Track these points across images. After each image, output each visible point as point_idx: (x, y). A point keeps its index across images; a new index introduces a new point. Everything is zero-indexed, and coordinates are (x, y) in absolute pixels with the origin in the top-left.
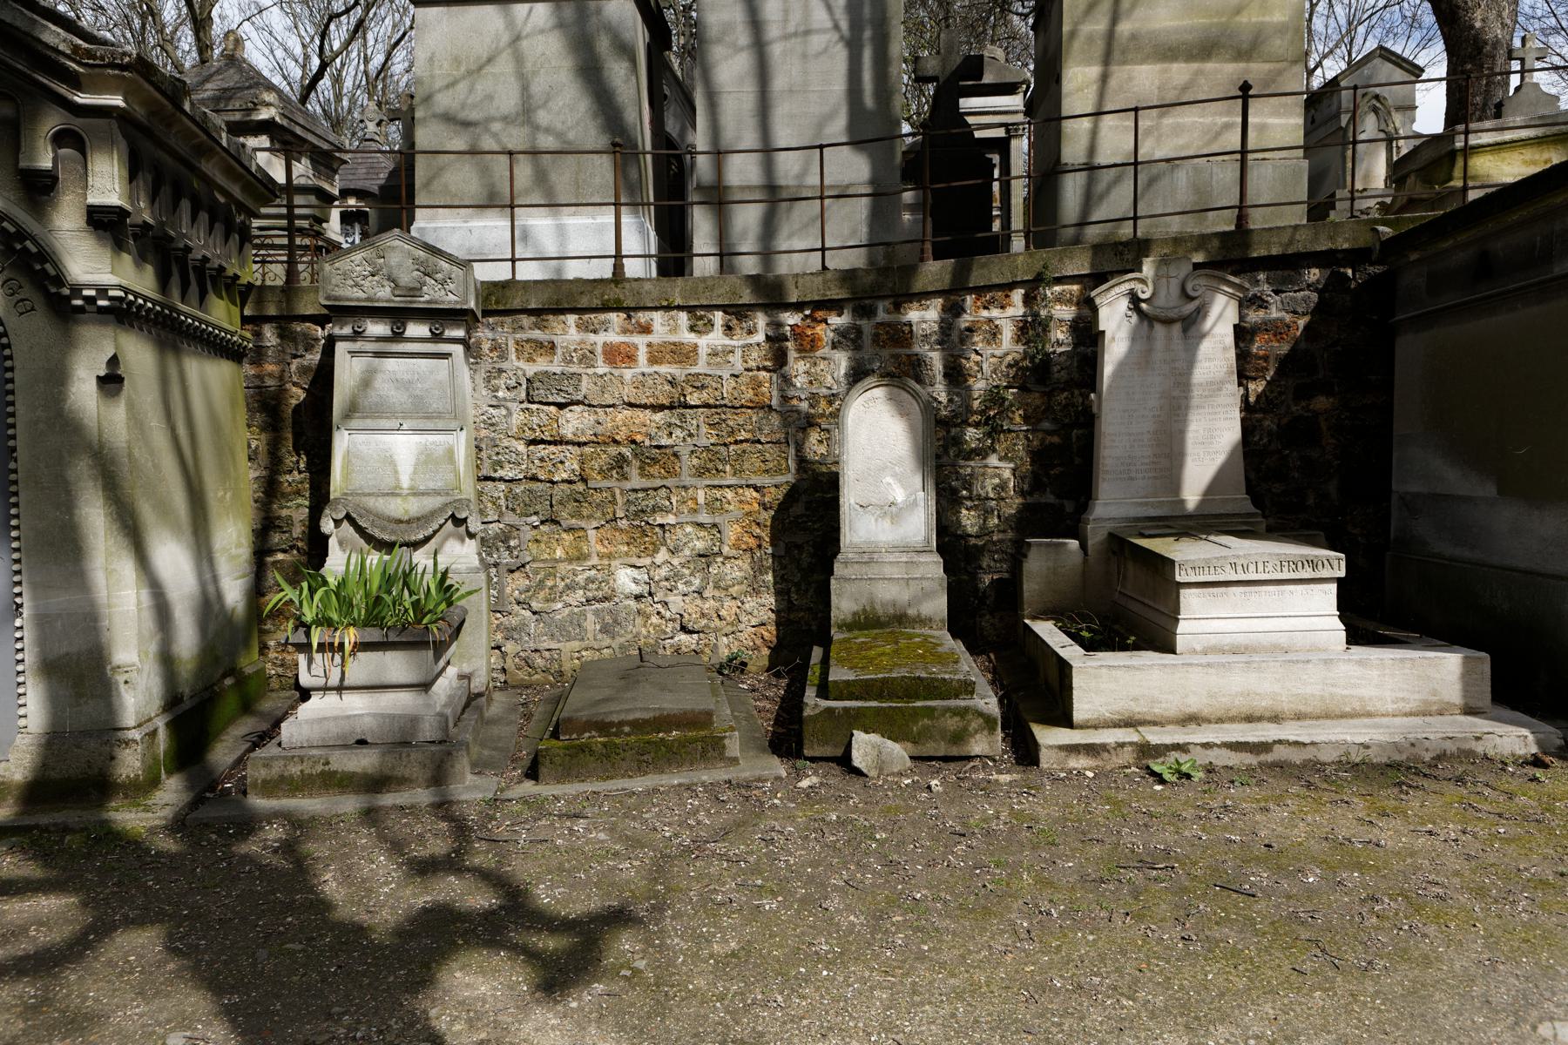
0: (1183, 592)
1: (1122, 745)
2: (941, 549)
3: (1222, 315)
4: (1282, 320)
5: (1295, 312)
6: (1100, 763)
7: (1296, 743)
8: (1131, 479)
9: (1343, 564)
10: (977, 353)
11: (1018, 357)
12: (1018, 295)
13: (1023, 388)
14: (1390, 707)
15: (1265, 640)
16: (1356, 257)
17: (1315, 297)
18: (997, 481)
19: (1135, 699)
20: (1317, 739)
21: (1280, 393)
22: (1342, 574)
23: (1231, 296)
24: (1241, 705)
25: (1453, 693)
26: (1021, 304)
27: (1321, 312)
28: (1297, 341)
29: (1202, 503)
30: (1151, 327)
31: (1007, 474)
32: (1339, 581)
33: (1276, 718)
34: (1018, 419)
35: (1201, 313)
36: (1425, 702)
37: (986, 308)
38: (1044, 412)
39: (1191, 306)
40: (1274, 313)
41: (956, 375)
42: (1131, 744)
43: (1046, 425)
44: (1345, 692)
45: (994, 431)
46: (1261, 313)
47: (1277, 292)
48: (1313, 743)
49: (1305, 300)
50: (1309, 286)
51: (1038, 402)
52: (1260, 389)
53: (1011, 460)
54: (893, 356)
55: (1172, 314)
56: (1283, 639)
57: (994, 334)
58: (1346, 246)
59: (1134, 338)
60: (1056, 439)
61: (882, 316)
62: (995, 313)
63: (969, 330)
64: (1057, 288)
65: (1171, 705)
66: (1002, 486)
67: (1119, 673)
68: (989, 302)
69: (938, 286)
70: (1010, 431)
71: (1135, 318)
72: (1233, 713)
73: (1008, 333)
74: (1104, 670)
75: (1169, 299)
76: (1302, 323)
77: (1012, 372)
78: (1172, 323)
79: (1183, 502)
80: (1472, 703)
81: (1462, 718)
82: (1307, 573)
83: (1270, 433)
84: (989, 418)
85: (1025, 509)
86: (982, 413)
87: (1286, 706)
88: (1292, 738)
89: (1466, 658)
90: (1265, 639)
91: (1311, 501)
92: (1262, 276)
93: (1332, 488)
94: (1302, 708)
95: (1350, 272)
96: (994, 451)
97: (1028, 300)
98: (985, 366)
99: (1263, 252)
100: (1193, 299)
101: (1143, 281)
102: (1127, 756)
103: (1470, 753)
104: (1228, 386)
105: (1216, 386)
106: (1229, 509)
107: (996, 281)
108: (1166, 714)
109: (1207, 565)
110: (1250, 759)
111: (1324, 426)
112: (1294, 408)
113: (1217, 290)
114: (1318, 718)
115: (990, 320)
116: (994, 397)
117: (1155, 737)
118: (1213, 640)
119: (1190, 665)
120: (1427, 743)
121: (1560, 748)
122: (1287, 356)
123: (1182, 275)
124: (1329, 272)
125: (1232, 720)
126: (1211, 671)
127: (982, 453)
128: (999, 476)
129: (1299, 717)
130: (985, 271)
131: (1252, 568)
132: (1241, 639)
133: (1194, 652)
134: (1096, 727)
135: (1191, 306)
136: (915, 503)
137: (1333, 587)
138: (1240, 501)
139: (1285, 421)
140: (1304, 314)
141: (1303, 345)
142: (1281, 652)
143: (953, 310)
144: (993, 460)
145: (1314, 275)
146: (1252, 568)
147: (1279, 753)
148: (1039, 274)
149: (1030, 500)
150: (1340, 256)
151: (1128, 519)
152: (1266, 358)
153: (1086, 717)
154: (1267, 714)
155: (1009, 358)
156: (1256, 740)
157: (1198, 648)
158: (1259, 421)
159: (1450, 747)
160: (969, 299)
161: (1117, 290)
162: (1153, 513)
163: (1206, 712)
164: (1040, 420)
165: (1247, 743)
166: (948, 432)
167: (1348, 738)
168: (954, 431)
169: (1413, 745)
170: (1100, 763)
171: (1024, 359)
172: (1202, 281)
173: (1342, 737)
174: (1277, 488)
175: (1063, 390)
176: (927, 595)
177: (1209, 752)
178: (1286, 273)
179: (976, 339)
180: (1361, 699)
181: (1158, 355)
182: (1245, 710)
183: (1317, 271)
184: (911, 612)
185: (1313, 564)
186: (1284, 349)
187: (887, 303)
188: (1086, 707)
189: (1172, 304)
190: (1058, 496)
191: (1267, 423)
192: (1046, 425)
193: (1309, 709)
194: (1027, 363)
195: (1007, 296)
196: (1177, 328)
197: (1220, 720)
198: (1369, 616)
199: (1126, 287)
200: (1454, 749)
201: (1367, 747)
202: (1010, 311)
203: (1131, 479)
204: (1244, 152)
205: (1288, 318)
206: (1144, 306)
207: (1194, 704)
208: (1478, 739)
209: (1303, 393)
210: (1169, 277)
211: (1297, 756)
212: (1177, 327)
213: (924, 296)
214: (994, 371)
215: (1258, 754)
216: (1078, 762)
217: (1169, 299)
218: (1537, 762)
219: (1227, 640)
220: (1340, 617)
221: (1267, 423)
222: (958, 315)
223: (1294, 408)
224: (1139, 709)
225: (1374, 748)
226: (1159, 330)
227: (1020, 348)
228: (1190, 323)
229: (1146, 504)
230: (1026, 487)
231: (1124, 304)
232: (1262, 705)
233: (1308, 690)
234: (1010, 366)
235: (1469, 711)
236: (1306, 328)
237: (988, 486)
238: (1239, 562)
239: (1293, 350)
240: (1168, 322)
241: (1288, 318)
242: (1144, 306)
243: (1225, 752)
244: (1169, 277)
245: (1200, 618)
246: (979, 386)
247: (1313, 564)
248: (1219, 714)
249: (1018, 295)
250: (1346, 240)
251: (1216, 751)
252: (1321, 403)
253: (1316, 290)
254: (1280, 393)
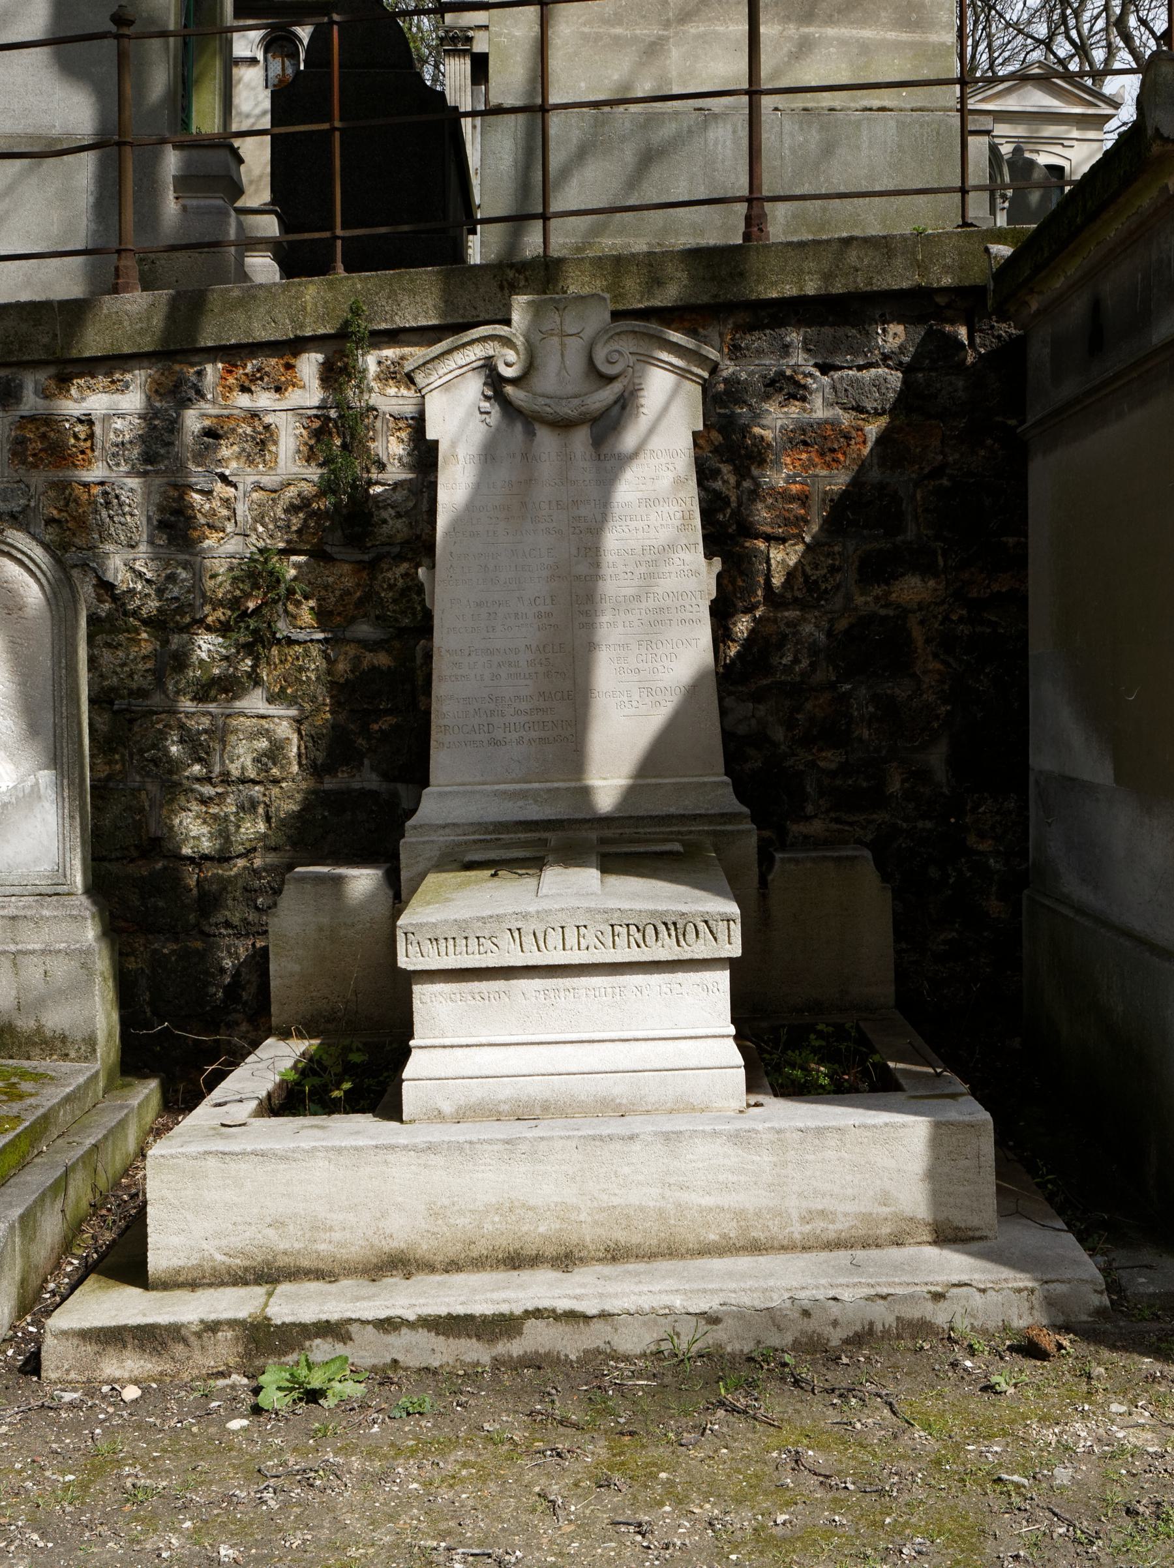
0: (417, 989)
1: (212, 1327)
2: (100, 886)
3: (667, 410)
4: (833, 423)
5: (859, 409)
6: (169, 1367)
7: (572, 1316)
8: (496, 743)
9: (737, 929)
10: (224, 478)
11: (308, 489)
12: (309, 365)
13: (319, 555)
14: (798, 1230)
15: (584, 1088)
16: (968, 301)
17: (895, 378)
18: (263, 744)
19: (278, 1224)
20: (612, 1306)
21: (833, 570)
22: (735, 950)
23: (682, 373)
24: (497, 1232)
25: (913, 1199)
26: (316, 383)
27: (909, 403)
28: (863, 467)
29: (631, 793)
30: (530, 433)
31: (284, 730)
32: (733, 964)
33: (566, 1260)
34: (306, 616)
35: (626, 404)
36: (866, 1218)
37: (245, 389)
38: (360, 602)
39: (607, 394)
40: (819, 410)
41: (176, 527)
42: (233, 1323)
43: (364, 630)
44: (708, 1201)
45: (255, 638)
46: (794, 410)
47: (825, 369)
48: (604, 1315)
49: (877, 384)
50: (885, 357)
51: (348, 583)
52: (792, 561)
53: (292, 701)
54: (53, 485)
55: (568, 410)
56: (618, 1087)
57: (262, 442)
58: (947, 281)
59: (489, 455)
60: (382, 660)
61: (31, 402)
62: (264, 400)
63: (211, 433)
64: (390, 353)
65: (352, 1233)
66: (275, 752)
67: (243, 1167)
68: (253, 380)
69: (147, 344)
70: (290, 642)
71: (496, 411)
72: (480, 1249)
73: (289, 440)
74: (212, 1162)
75: (560, 377)
76: (872, 429)
77: (296, 522)
78: (563, 428)
79: (585, 793)
80: (961, 1218)
81: (932, 1252)
82: (665, 950)
83: (814, 650)
84: (244, 614)
85: (314, 802)
86: (234, 603)
87: (590, 1234)
88: (563, 1305)
89: (937, 1125)
90: (592, 1089)
91: (895, 785)
92: (794, 337)
93: (936, 758)
94: (621, 1236)
95: (963, 332)
96: (257, 682)
97: (335, 375)
98: (241, 508)
99: (790, 290)
100: (610, 379)
101: (507, 342)
102: (224, 1350)
103: (922, 1328)
104: (687, 556)
105: (654, 560)
106: (687, 805)
107: (262, 334)
108: (343, 1254)
109: (462, 932)
110: (475, 1351)
111: (918, 634)
112: (860, 600)
113: (649, 360)
114: (652, 1256)
115: (254, 415)
116: (255, 573)
117: (291, 1305)
118: (478, 1091)
119: (392, 1148)
120: (835, 1310)
121: (1100, 1312)
122: (845, 494)
123: (589, 332)
124: (921, 331)
125: (478, 1263)
126: (433, 1160)
127: (228, 687)
128: (266, 733)
129: (615, 1255)
130: (240, 317)
131: (554, 938)
132: (535, 1089)
133: (439, 1117)
134: (193, 1285)
135: (607, 394)
136: (34, 794)
137: (723, 978)
138: (710, 788)
139: (842, 624)
140: (878, 414)
141: (875, 475)
142: (604, 1115)
143: (174, 394)
144: (255, 702)
145: (894, 336)
146: (554, 938)
147: (537, 1338)
148: (347, 323)
149: (329, 784)
150: (941, 300)
151: (481, 827)
152: (803, 499)
153: (176, 1262)
154: (550, 1251)
155: (292, 492)
156: (443, 1311)
157: (447, 1108)
158: (792, 624)
159: (884, 1316)
160: (212, 372)
161: (460, 358)
162: (534, 812)
163: (424, 1248)
164: (352, 620)
165: (469, 1318)
166: (166, 642)
167: (678, 1302)
168: (176, 640)
169: (806, 1313)
170: (169, 1367)
171: (322, 494)
172: (627, 345)
173: (666, 1300)
174: (830, 759)
175: (400, 558)
176: (78, 988)
177: (391, 1339)
178: (841, 332)
179: (225, 452)
180: (739, 1214)
181: (545, 492)
182: (506, 1243)
183: (900, 329)
184: (26, 1024)
185: (676, 927)
186: (839, 481)
187: (42, 376)
188: (175, 1240)
189: (570, 389)
190: (386, 776)
191: (808, 628)
192: (364, 630)
193: (636, 1239)
194: (324, 504)
195: (289, 367)
196: (581, 438)
197: (453, 1266)
198: (795, 1040)
199: (475, 353)
200: (890, 1320)
201: (713, 1319)
202: (295, 398)
203: (496, 743)
204: (754, 92)
205: (846, 419)
206: (509, 389)
207: (401, 1230)
208: (938, 1297)
209: (878, 570)
210: (563, 335)
211: (570, 1343)
212: (581, 438)
213: (110, 365)
214: (260, 519)
215: (492, 1339)
216: (126, 1368)
217: (560, 377)
218: (1030, 1350)
219: (505, 1091)
220: (737, 1038)
221: (808, 628)
222: (185, 403)
223: (860, 600)
224: (286, 1244)
225: (728, 1322)
226: (546, 440)
227: (314, 473)
228: (604, 425)
229: (523, 795)
230: (321, 756)
231: (473, 387)
232: (538, 1231)
233: (635, 1197)
234: (292, 509)
235: (947, 1235)
236: (881, 440)
237: (242, 757)
238: (528, 928)
239: (856, 482)
240: (563, 425)
241: (846, 419)
242: (509, 389)
243: (423, 1337)
244: (563, 335)
245: (453, 1045)
246: (223, 550)
247: (676, 927)
248: (453, 1251)
249: (309, 365)
250: (947, 269)
251: (406, 1336)
252: (912, 589)
253: (899, 366)
254: (833, 570)
